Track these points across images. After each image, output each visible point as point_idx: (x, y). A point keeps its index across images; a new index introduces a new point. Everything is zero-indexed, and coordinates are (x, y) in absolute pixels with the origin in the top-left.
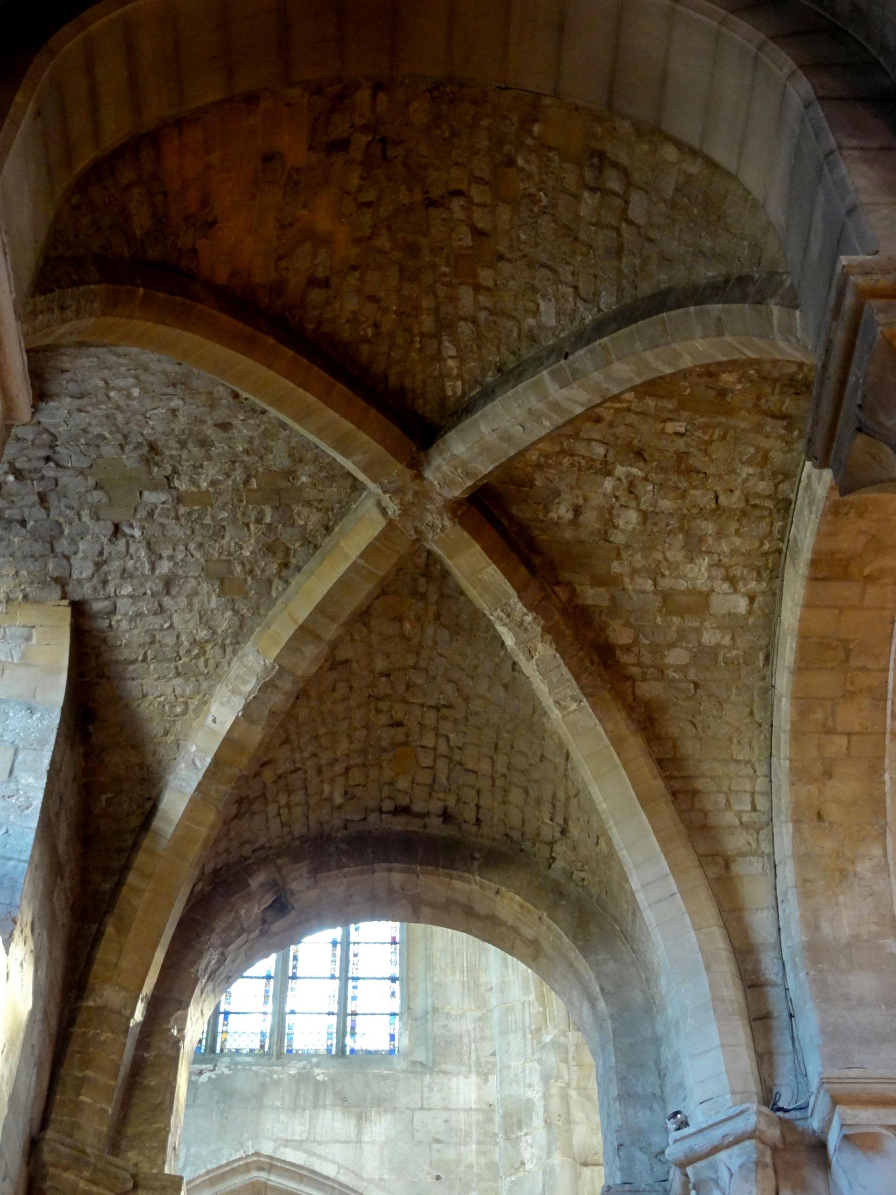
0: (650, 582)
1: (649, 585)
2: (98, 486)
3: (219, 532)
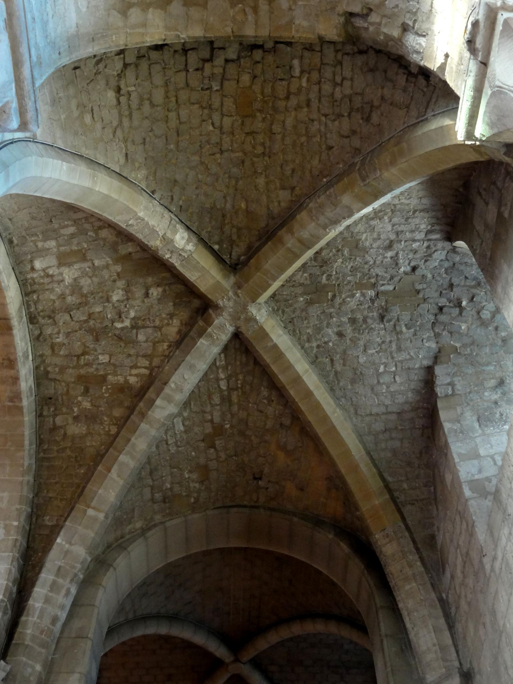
0: (96, 264)
1: (97, 263)
2: (418, 292)
3: (354, 270)
